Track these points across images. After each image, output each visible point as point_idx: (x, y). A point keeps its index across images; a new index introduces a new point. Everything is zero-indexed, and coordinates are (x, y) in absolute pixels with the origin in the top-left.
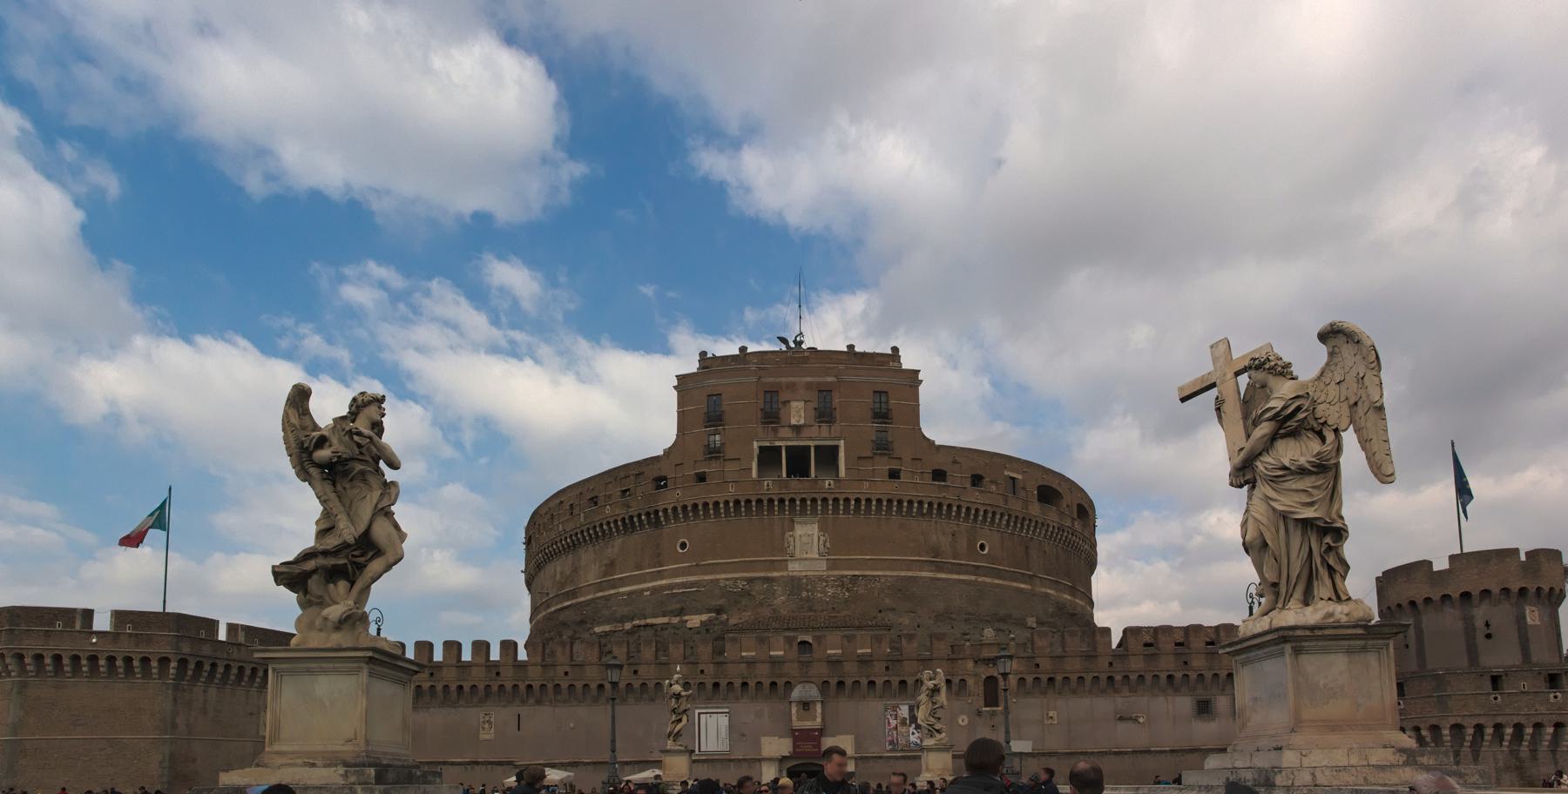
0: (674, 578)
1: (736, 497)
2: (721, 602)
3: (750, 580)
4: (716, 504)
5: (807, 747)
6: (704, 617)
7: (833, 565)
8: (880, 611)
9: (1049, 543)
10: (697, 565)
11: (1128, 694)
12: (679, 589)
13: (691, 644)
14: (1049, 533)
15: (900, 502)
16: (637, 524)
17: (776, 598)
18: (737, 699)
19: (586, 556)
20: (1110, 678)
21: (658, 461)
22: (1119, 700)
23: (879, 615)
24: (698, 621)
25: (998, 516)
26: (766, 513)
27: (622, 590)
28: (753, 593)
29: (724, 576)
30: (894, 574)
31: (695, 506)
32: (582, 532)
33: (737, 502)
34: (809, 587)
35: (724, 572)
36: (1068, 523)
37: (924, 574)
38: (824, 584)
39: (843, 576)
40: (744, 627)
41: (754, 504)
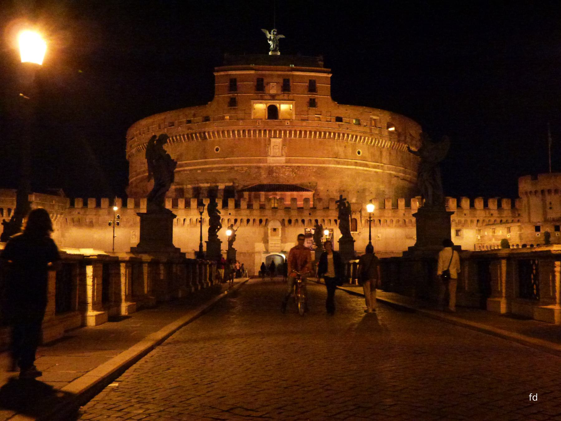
3: (250, 167)
4: (233, 131)
6: (227, 184)
11: (412, 227)
12: (215, 170)
14: (392, 145)
16: (194, 137)
17: (261, 176)
18: (245, 226)
20: (405, 221)
24: (224, 186)
25: (367, 138)
26: (257, 135)
28: (251, 174)
31: (223, 132)
33: (244, 131)
36: (403, 138)
37: (331, 166)
38: (284, 170)
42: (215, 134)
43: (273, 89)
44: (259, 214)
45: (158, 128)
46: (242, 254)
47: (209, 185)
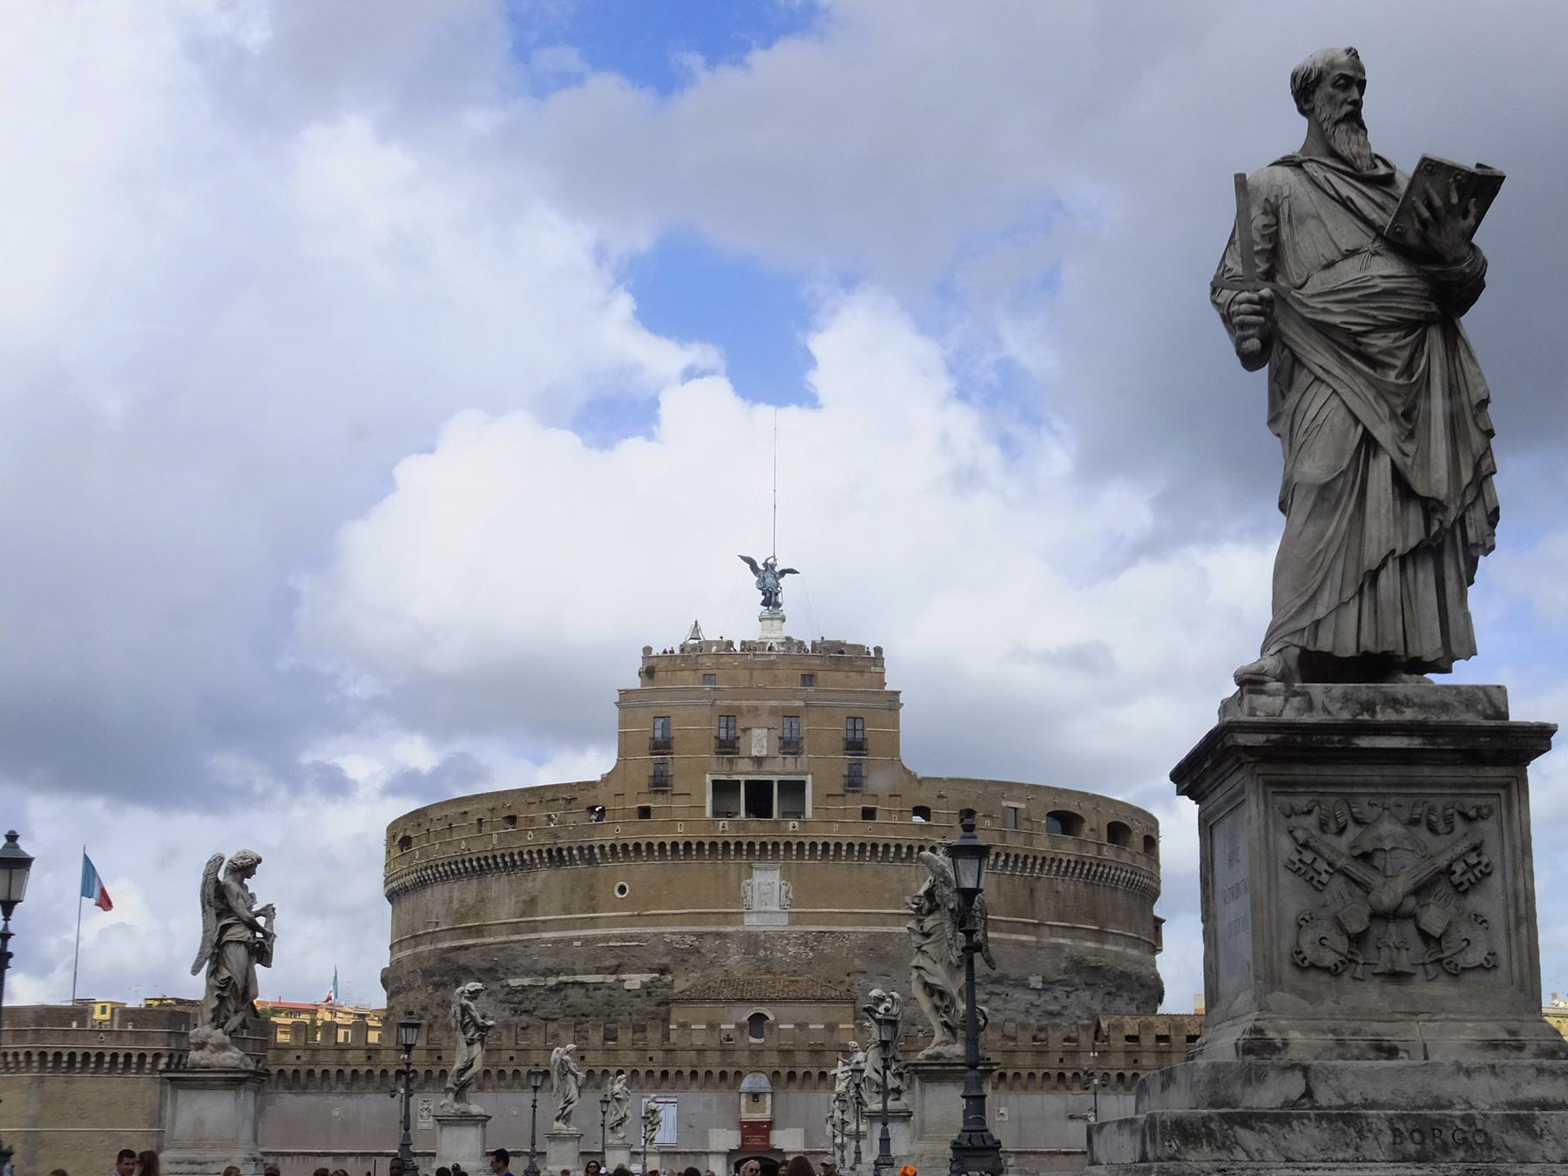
0: (610, 927)
1: (687, 839)
2: (666, 960)
3: (700, 935)
5: (756, 1141)
6: (646, 977)
7: (796, 919)
8: (848, 975)
9: (1063, 880)
10: (639, 915)
11: (1079, 1092)
13: (629, 1009)
14: (1063, 869)
15: (874, 846)
16: (567, 858)
17: (729, 958)
18: (686, 1088)
19: (498, 886)
20: (1061, 1076)
21: (594, 788)
22: (1070, 1097)
23: (847, 979)
27: (545, 935)
28: (703, 951)
29: (670, 929)
30: (867, 929)
31: (637, 846)
32: (494, 857)
33: (688, 845)
34: (768, 945)
35: (669, 925)
38: (785, 941)
39: (806, 932)
40: (693, 996)
41: (707, 847)
42: (617, 853)
43: (759, 742)
44: (719, 1060)
45: (475, 829)
46: (678, 1157)
47: (598, 978)
